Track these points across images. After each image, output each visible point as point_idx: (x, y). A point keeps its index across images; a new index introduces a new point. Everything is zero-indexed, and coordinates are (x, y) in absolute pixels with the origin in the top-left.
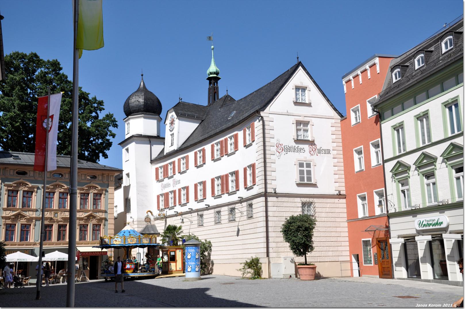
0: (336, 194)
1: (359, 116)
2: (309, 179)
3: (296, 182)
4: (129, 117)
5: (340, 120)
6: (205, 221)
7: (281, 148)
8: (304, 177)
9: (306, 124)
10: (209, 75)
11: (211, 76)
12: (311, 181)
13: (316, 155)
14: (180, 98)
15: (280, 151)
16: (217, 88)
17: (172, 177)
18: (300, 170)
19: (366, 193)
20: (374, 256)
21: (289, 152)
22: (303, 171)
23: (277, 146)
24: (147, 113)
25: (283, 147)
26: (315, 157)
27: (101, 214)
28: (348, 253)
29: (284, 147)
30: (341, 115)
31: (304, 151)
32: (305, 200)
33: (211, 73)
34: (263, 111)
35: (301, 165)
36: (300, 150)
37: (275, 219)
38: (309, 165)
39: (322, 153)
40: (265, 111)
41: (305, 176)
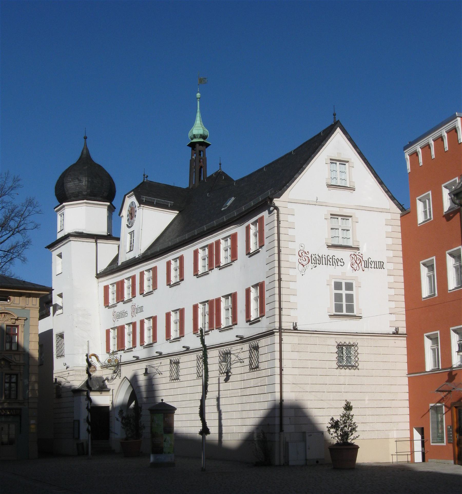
1: (430, 209)
2: (350, 308)
4: (64, 204)
5: (399, 215)
6: (262, 358)
7: (306, 258)
10: (192, 139)
11: (195, 140)
12: (353, 311)
13: (361, 269)
14: (144, 175)
15: (304, 263)
16: (205, 160)
17: (130, 300)
18: (336, 294)
19: (438, 332)
20: (448, 431)
21: (319, 264)
22: (341, 294)
23: (301, 255)
25: (309, 256)
28: (408, 426)
29: (311, 257)
30: (401, 208)
31: (342, 264)
33: (195, 136)
34: (279, 197)
35: (338, 286)
36: (336, 262)
37: (296, 371)
38: (349, 286)
39: (371, 268)
41: (344, 303)
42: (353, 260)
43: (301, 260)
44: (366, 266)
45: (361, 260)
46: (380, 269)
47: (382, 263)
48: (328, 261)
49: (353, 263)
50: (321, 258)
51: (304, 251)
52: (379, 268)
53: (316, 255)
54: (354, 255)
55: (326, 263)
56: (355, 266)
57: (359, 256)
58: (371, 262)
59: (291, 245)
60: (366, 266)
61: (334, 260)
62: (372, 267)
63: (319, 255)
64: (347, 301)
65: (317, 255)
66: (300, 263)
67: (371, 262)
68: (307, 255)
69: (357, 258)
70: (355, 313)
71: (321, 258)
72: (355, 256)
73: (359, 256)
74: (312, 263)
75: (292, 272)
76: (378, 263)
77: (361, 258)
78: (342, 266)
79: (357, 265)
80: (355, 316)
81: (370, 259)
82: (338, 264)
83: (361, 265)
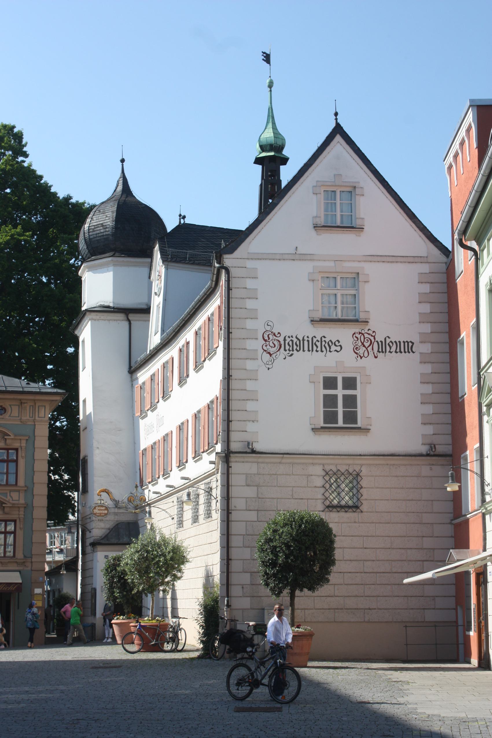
0: (425, 453)
7: (276, 343)
12: (356, 422)
15: (272, 350)
18: (325, 396)
21: (298, 351)
22: (336, 396)
23: (266, 338)
25: (281, 339)
26: (369, 362)
29: (285, 340)
31: (338, 349)
39: (391, 352)
41: (340, 410)
42: (357, 342)
43: (266, 346)
44: (380, 350)
45: (373, 340)
46: (403, 353)
47: (410, 344)
48: (314, 346)
49: (357, 346)
51: (272, 332)
52: (405, 352)
53: (292, 337)
54: (360, 333)
55: (310, 349)
56: (362, 350)
57: (369, 334)
58: (391, 344)
59: (250, 324)
61: (323, 343)
62: (391, 351)
63: (297, 337)
65: (294, 337)
66: (265, 351)
67: (391, 344)
68: (277, 338)
69: (364, 338)
70: (359, 425)
72: (361, 334)
73: (369, 334)
74: (285, 350)
75: (250, 365)
76: (402, 344)
77: (372, 338)
78: (338, 352)
79: (365, 349)
80: (359, 428)
81: (389, 338)
82: (330, 348)
83: (373, 349)
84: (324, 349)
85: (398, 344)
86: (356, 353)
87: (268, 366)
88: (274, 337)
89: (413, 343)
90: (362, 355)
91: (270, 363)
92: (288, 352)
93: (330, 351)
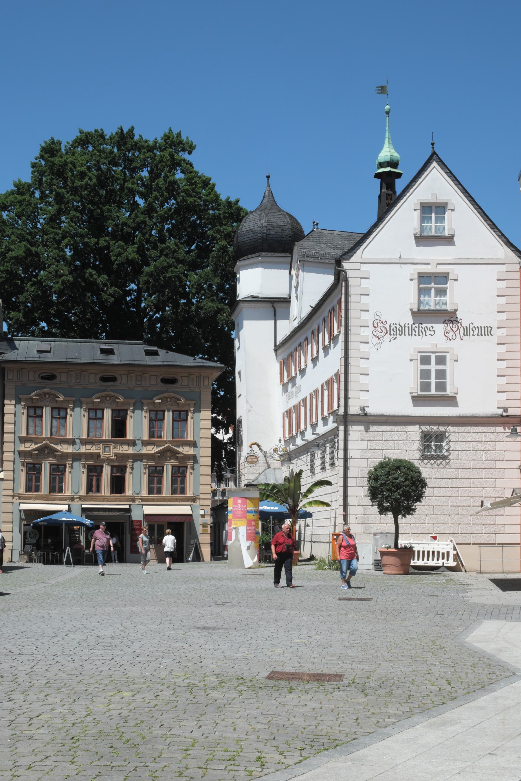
2: (441, 386)
3: (411, 393)
7: (383, 329)
8: (430, 383)
9: (444, 277)
12: (445, 390)
15: (380, 335)
18: (422, 371)
21: (400, 335)
23: (376, 325)
24: (270, 254)
25: (387, 326)
27: (186, 448)
29: (390, 327)
31: (432, 333)
32: (426, 428)
34: (348, 259)
35: (425, 360)
38: (441, 360)
39: (474, 335)
40: (353, 259)
41: (433, 381)
44: (465, 334)
47: (489, 329)
48: (413, 331)
50: (403, 328)
52: (485, 335)
53: (396, 324)
55: (410, 333)
58: (474, 329)
60: (465, 334)
61: (421, 329)
64: (437, 378)
67: (474, 329)
68: (384, 325)
70: (449, 392)
71: (403, 328)
74: (390, 335)
76: (483, 329)
78: (432, 335)
81: (473, 324)
84: (421, 333)
85: (479, 328)
86: (446, 336)
87: (377, 347)
88: (382, 325)
89: (491, 328)
90: (451, 338)
91: (379, 345)
92: (392, 336)
93: (426, 335)
